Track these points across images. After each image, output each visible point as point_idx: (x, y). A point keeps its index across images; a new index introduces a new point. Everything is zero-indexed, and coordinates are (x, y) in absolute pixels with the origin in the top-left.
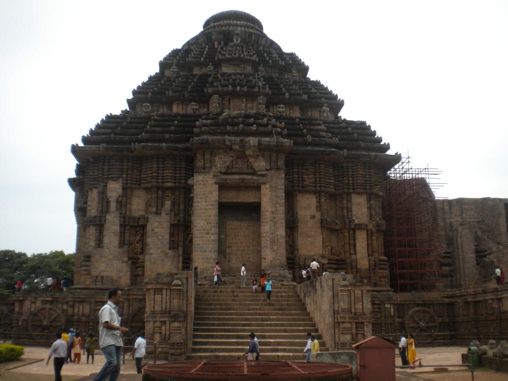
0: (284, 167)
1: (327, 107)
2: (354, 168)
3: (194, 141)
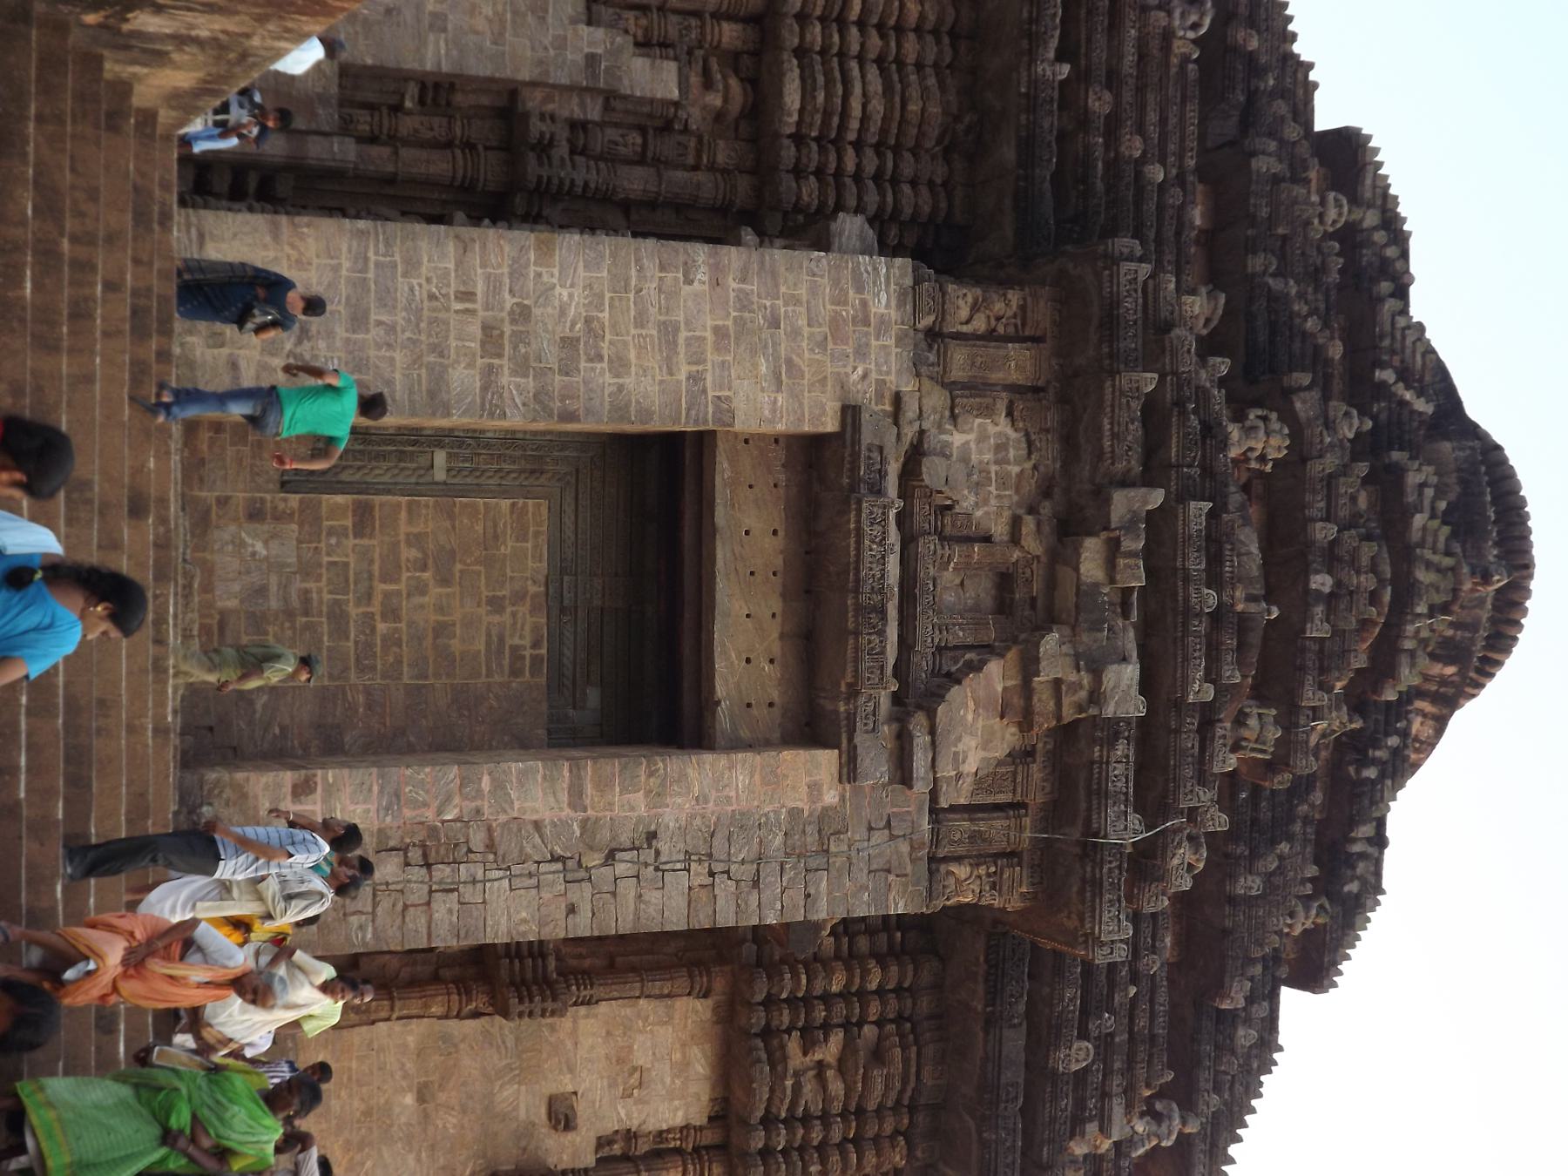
3: (1126, 266)
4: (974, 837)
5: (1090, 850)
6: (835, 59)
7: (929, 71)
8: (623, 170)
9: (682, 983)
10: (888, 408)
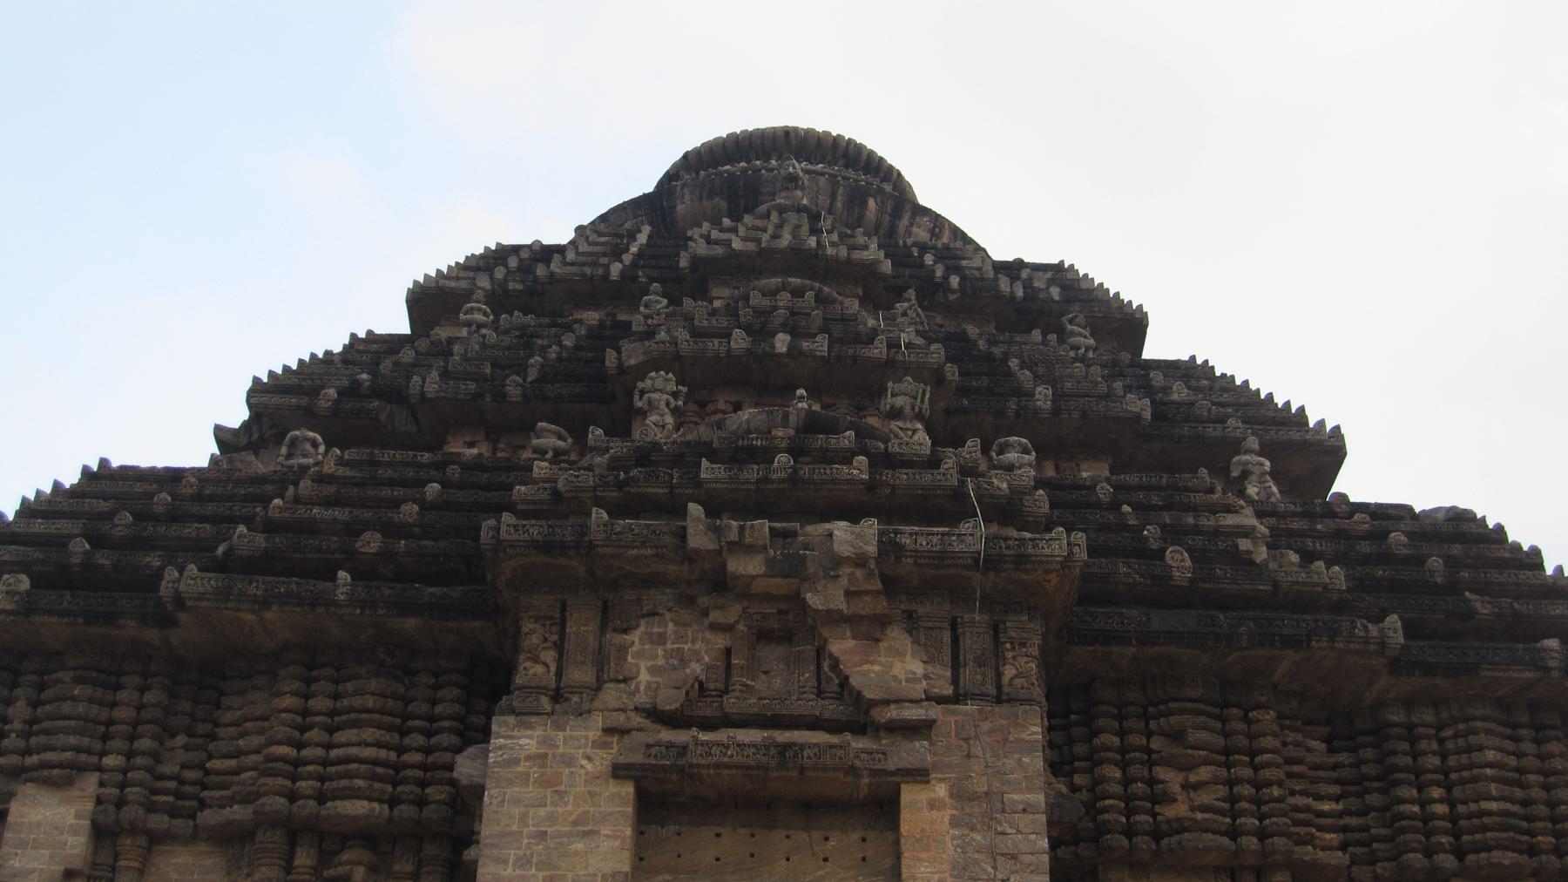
0: (1038, 692)
1: (1260, 454)
2: (1448, 733)
3: (504, 535)
4: (980, 662)
5: (990, 563)
6: (328, 769)
7: (341, 688)
10: (615, 739)
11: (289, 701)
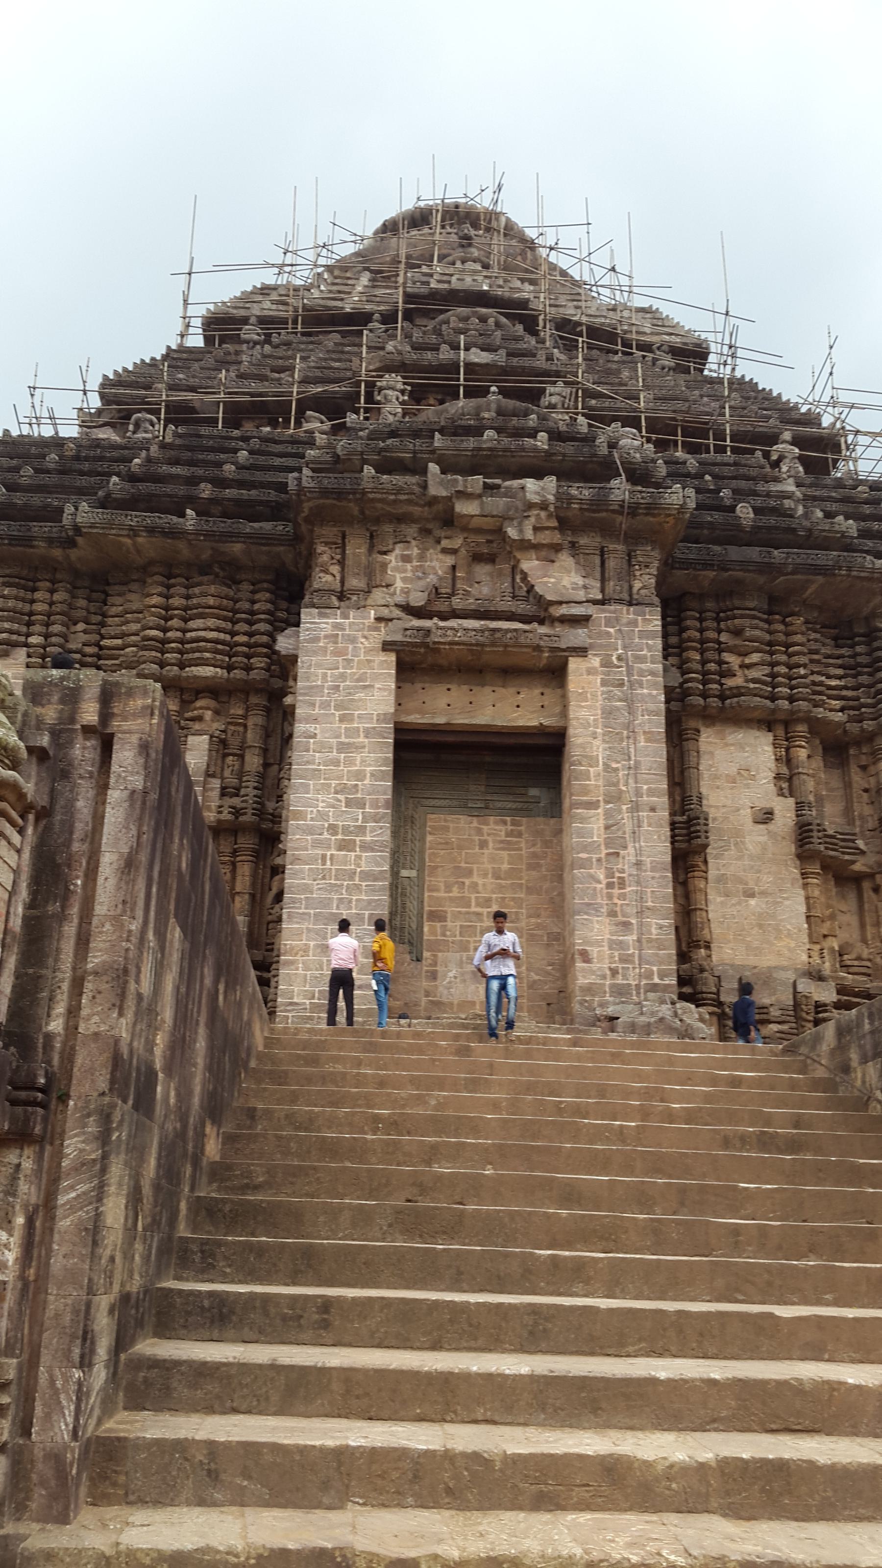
7: (190, 592)
8: (247, 768)
9: (690, 745)
11: (156, 600)
